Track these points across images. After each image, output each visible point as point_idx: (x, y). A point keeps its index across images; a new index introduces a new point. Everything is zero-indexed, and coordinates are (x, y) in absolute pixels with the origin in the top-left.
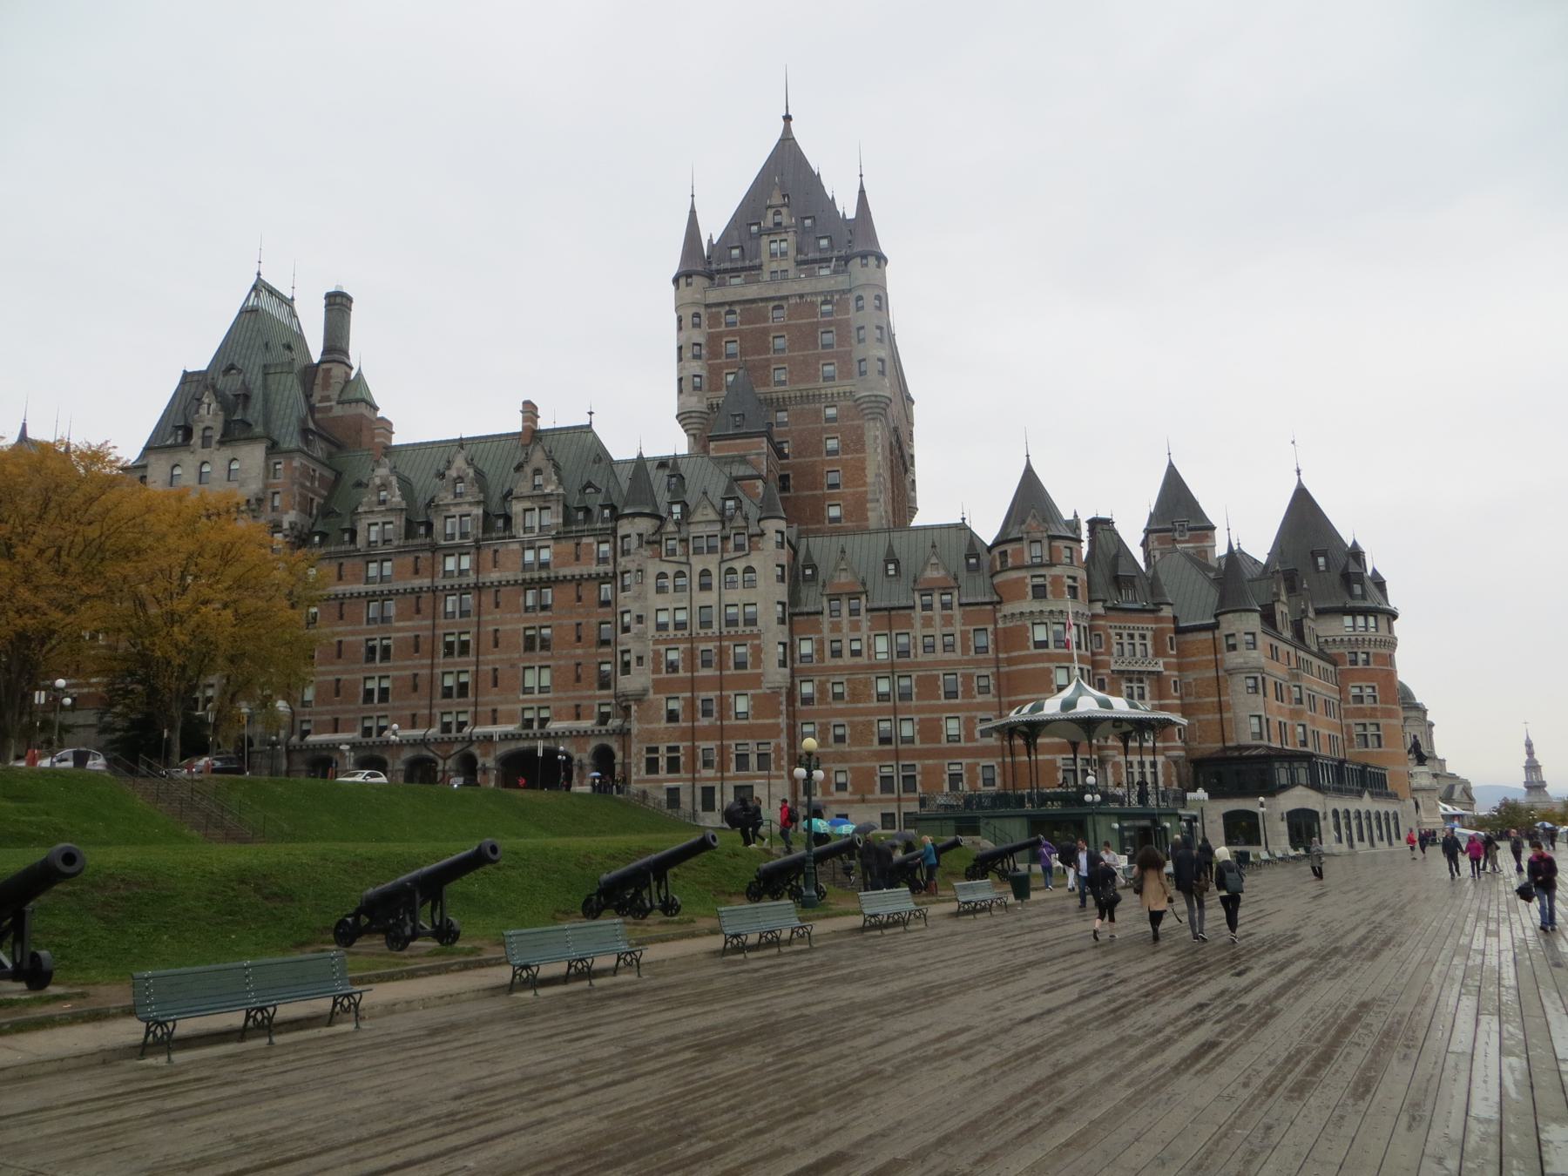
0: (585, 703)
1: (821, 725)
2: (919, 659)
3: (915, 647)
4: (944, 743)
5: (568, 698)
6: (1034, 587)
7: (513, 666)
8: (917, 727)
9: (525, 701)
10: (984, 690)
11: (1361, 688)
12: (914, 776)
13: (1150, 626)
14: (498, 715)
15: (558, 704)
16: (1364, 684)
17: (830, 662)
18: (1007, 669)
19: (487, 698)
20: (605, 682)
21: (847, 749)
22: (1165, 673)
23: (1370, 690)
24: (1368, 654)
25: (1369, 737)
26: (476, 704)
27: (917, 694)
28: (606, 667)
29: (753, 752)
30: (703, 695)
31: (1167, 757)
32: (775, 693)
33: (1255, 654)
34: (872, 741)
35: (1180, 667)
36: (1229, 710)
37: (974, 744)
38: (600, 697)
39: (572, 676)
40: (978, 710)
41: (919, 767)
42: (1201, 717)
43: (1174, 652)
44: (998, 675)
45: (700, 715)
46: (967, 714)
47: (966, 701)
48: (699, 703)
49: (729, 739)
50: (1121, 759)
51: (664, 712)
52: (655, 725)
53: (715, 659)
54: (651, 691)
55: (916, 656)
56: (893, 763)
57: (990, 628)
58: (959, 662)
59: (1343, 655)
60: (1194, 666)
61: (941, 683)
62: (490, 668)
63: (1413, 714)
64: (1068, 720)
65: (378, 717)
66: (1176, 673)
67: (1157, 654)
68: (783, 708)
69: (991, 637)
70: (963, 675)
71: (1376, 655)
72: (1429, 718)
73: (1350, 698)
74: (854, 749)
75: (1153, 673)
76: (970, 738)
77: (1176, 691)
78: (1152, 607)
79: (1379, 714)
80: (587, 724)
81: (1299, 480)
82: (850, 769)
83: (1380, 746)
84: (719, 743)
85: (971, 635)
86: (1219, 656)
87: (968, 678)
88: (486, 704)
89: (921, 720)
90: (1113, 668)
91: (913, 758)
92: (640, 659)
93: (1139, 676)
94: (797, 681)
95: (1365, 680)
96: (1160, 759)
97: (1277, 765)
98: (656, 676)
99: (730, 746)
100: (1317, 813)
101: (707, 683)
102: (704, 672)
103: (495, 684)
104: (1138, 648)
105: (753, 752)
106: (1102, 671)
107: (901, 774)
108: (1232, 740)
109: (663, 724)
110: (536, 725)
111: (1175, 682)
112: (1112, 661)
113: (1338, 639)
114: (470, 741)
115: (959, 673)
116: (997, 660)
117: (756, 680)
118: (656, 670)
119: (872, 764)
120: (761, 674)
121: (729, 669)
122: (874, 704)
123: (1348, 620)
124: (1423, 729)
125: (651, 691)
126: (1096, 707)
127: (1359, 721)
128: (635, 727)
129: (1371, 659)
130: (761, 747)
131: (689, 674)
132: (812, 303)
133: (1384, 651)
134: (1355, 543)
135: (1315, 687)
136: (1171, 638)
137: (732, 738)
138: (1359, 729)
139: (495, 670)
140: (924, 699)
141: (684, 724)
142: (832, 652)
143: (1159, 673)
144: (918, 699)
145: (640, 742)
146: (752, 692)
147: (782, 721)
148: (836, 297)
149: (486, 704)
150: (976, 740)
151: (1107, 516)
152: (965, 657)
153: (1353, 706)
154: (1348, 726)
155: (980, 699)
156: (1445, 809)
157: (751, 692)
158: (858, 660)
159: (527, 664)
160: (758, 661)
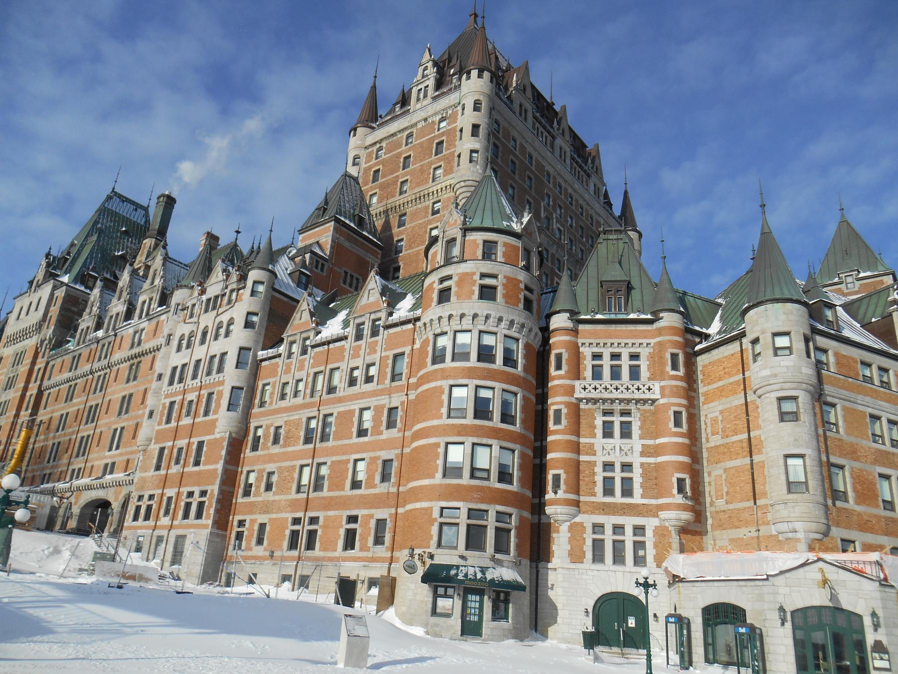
22: (662, 401)
29: (195, 500)
40: (382, 449)
75: (645, 401)
86: (747, 374)
90: (576, 395)
100: (860, 617)
108: (764, 495)
109: (152, 472)
132: (433, 122)
148: (450, 112)
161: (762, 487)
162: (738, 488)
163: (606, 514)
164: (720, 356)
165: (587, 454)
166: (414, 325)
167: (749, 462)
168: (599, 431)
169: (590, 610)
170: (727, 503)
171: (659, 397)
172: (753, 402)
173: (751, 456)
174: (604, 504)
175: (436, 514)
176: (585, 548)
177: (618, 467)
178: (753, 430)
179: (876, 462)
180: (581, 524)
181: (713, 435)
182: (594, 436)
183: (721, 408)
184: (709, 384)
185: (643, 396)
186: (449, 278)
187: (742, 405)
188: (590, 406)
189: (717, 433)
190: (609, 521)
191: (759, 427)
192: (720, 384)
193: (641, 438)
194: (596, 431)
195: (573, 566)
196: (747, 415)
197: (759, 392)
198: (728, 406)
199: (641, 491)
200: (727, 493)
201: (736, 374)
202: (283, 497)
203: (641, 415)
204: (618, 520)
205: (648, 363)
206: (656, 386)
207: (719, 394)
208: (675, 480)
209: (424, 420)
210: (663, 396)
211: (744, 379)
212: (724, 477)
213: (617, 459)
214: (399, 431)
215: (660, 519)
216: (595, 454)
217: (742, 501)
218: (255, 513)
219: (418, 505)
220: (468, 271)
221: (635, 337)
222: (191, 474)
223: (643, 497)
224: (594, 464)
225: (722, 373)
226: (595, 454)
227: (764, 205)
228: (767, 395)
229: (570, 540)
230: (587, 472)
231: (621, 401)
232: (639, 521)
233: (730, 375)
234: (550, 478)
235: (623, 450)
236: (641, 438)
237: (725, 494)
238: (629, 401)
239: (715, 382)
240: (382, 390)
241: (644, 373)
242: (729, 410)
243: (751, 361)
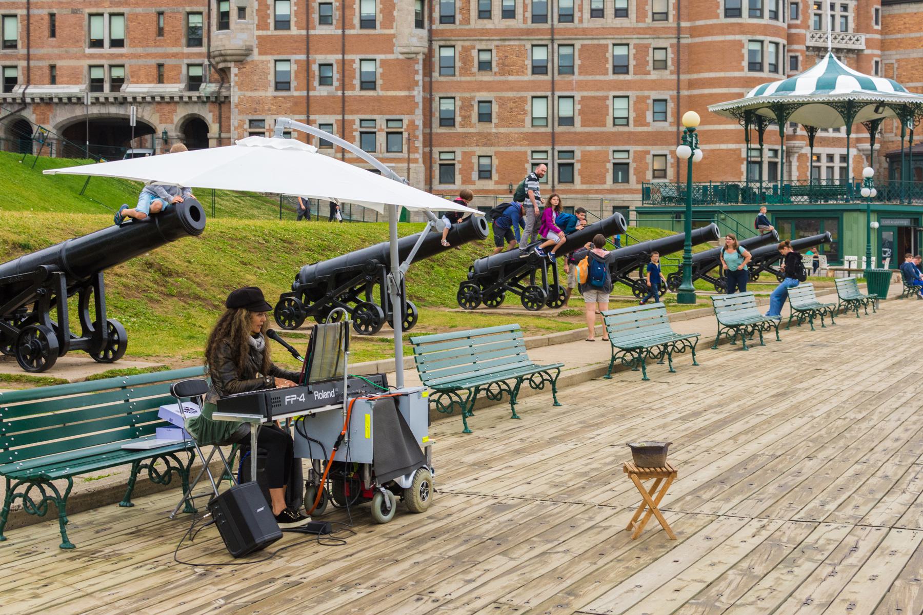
0: (168, 62)
1: (463, 100)
2: (585, 25)
3: (581, 10)
4: (609, 127)
5: (148, 55)
7: (75, 12)
8: (578, 107)
9: (91, 56)
10: (661, 65)
12: (572, 165)
14: (58, 72)
15: (134, 62)
17: (476, 23)
18: (689, 41)
19: (42, 51)
20: (194, 38)
21: (494, 130)
22: (867, 52)
26: (28, 58)
27: (580, 67)
28: (195, 20)
29: (381, 130)
30: (321, 58)
31: (859, 150)
32: (410, 59)
34: (523, 121)
35: (883, 46)
37: (645, 129)
38: (189, 56)
39: (153, 29)
40: (652, 89)
41: (578, 155)
43: (879, 27)
44: (678, 47)
45: (316, 83)
46: (639, 93)
47: (638, 77)
48: (315, 68)
49: (352, 113)
50: (807, 150)
51: (271, 77)
52: (260, 94)
53: (337, 14)
54: (256, 51)
55: (581, 21)
56: (549, 148)
58: (635, 31)
60: (899, 44)
61: (609, 55)
62: (44, 12)
64: (828, 103)
65: (111, 66)
66: (878, 52)
67: (858, 30)
68: (419, 77)
70: (636, 46)
74: (502, 130)
76: (640, 121)
80: (174, 88)
82: (496, 153)
84: (340, 117)
87: (642, 50)
88: (41, 58)
89: (583, 98)
91: (573, 143)
92: (242, 11)
94: (436, 45)
98: (261, 33)
99: (353, 121)
101: (327, 43)
102: (321, 30)
103: (53, 34)
104: (838, 20)
105: (381, 130)
107: (557, 161)
109: (271, 92)
110: (107, 86)
111: (877, 63)
112: (809, 35)
114: (24, 104)
115: (632, 43)
116: (679, 29)
117: (387, 43)
118: (262, 25)
119: (523, 149)
120: (394, 36)
121: (353, 27)
122: (528, 77)
125: (256, 51)
126: (858, 88)
128: (235, 95)
130: (391, 124)
131: (304, 32)
136: (877, 10)
137: (357, 112)
139: (52, 16)
140: (587, 73)
141: (296, 94)
142: (592, 11)
144: (580, 73)
145: (240, 113)
146: (382, 57)
147: (418, 94)
149: (41, 58)
150: (648, 125)
152: (641, 25)
155: (654, 75)
157: (379, 57)
158: (510, 23)
159: (94, 10)
160: (389, 20)
183: (898, 57)
185: (854, 47)
198: (906, 56)
202: (517, 130)
204: (830, 150)
206: (863, 37)
207: (897, 44)
209: (722, 70)
210: (868, 47)
214: (672, 73)
218: (468, 145)
222: (360, 99)
229: (799, 168)
233: (911, 31)
239: (894, 33)
241: (851, 25)
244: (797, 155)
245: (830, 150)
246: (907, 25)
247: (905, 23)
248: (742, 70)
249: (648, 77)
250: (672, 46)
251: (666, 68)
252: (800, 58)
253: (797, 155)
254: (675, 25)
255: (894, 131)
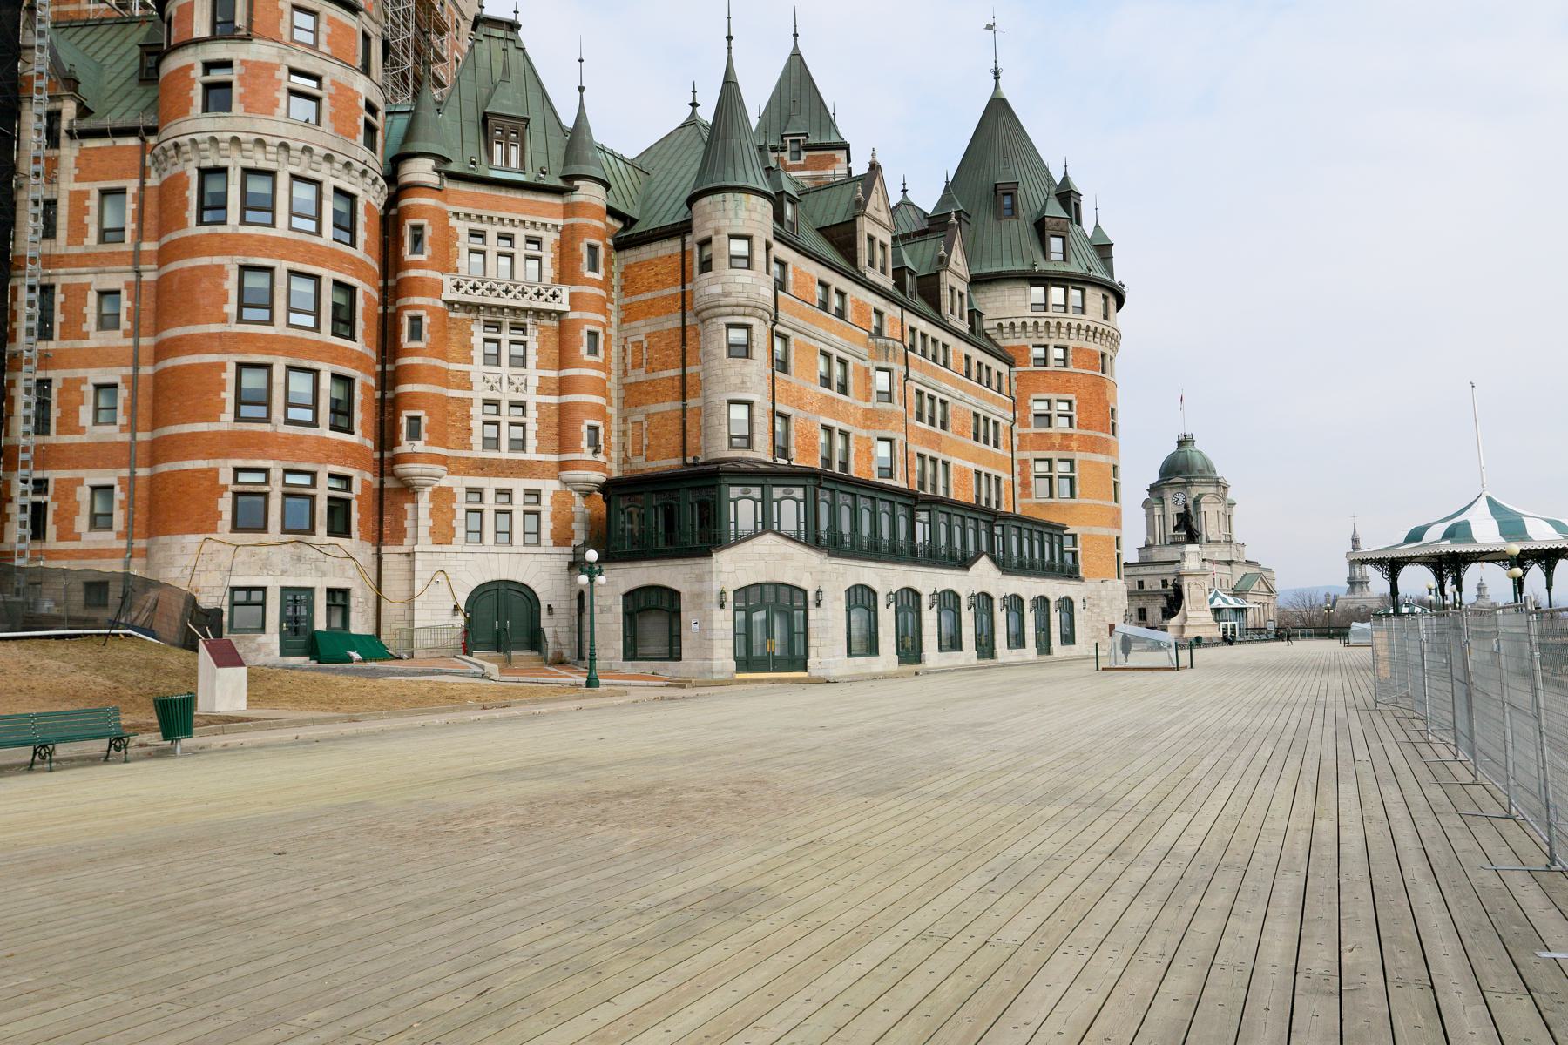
6: (208, 87)
11: (1049, 401)
13: (550, 221)
16: (1053, 396)
22: (572, 315)
23: (1065, 406)
24: (1065, 348)
25: (1055, 480)
33: (744, 276)
36: (696, 395)
40: (90, 365)
42: (655, 408)
43: (599, 276)
57: (132, 186)
59: (1024, 349)
63: (1211, 489)
69: (131, 206)
71: (1077, 350)
72: (1230, 495)
73: (1031, 418)
75: (548, 313)
77: (593, 350)
78: (559, 183)
79: (1074, 444)
81: (997, 86)
83: (1072, 495)
85: (93, 203)
86: (688, 287)
90: (447, 296)
93: (520, 318)
95: (1056, 390)
96: (549, 487)
97: (735, 492)
100: (805, 592)
106: (416, 300)
112: (448, 281)
113: (1018, 322)
123: (1037, 292)
124: (1221, 507)
127: (1040, 455)
129: (1070, 357)
133: (1096, 346)
134: (1066, 178)
135: (945, 386)
138: (1042, 467)
143: (560, 313)
150: (81, 430)
151: (510, 17)
153: (1033, 430)
154: (1024, 462)
156: (1225, 601)
161: (695, 441)
162: (663, 440)
163: (485, 475)
164: (652, 255)
165: (459, 387)
166: (142, 139)
167: (680, 407)
168: (477, 355)
169: (462, 606)
170: (646, 460)
171: (567, 308)
172: (694, 327)
173: (684, 400)
174: (483, 460)
175: (226, 477)
176: (455, 523)
177: (504, 407)
178: (690, 365)
179: (821, 411)
180: (449, 490)
181: (634, 367)
182: (470, 361)
183: (648, 330)
184: (633, 294)
186: (227, 64)
187: (678, 328)
188: (461, 315)
189: (641, 366)
190: (490, 484)
191: (698, 361)
192: (649, 295)
193: (538, 367)
194: (473, 353)
195: (437, 548)
196: (684, 343)
197: (705, 314)
198: (658, 328)
199: (536, 443)
200: (648, 447)
201: (673, 285)
203: (540, 333)
204: (504, 483)
205: (552, 255)
206: (565, 292)
207: (646, 308)
208: (584, 429)
211: (684, 294)
212: (645, 424)
213: (506, 395)
214: (126, 335)
215: (562, 481)
216: (470, 389)
217: (667, 457)
219: (188, 465)
220: (264, 58)
221: (535, 212)
223: (538, 450)
224: (468, 403)
225: (653, 280)
226: (470, 389)
227: (732, 38)
228: (714, 320)
230: (458, 414)
231: (514, 310)
232: (533, 484)
233: (665, 286)
234: (404, 421)
235: (513, 384)
236: (538, 367)
237: (644, 447)
238: (525, 311)
239: (641, 292)
240: (79, 256)
242: (658, 334)
243: (696, 271)
244: (429, 489)
245: (504, 483)
246: (660, 277)
247: (656, 274)
248: (225, 321)
249: (85, 344)
250: (128, 285)
251: (117, 327)
252: (427, 320)
253: (429, 489)
254: (131, 248)
255: (644, 453)
